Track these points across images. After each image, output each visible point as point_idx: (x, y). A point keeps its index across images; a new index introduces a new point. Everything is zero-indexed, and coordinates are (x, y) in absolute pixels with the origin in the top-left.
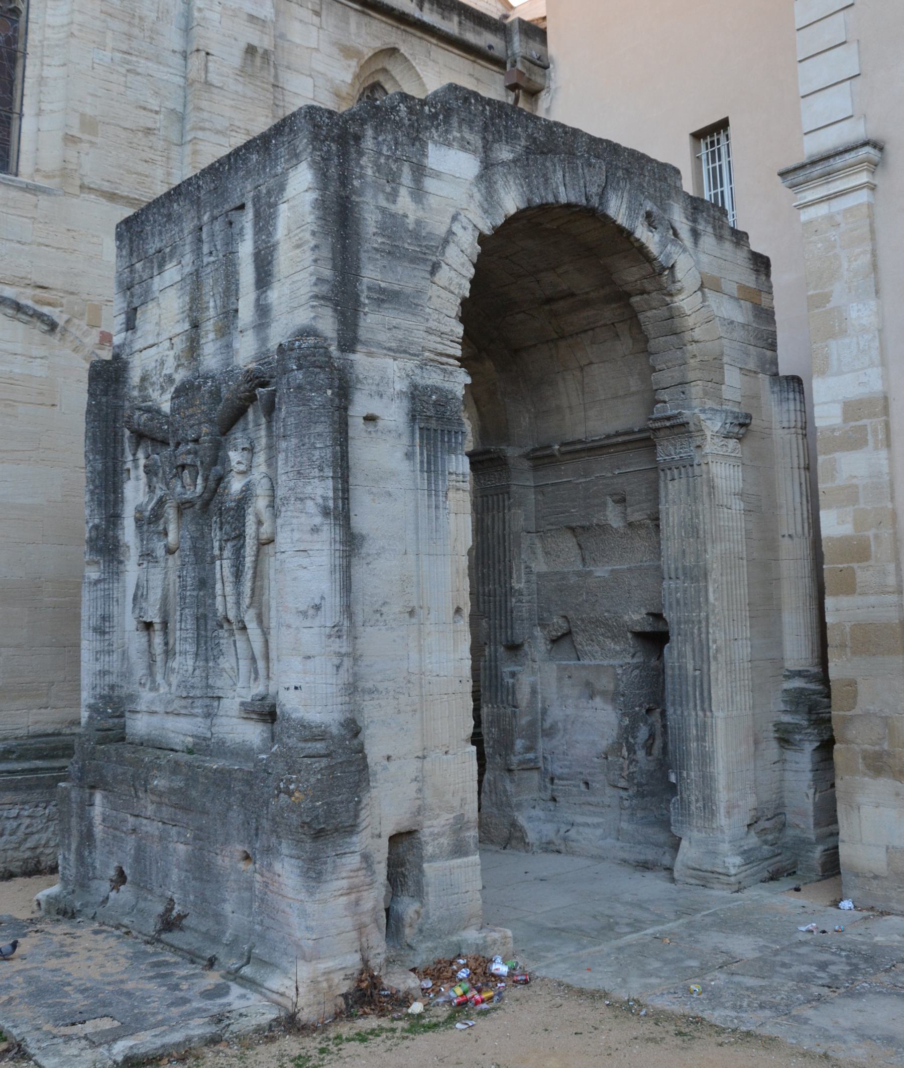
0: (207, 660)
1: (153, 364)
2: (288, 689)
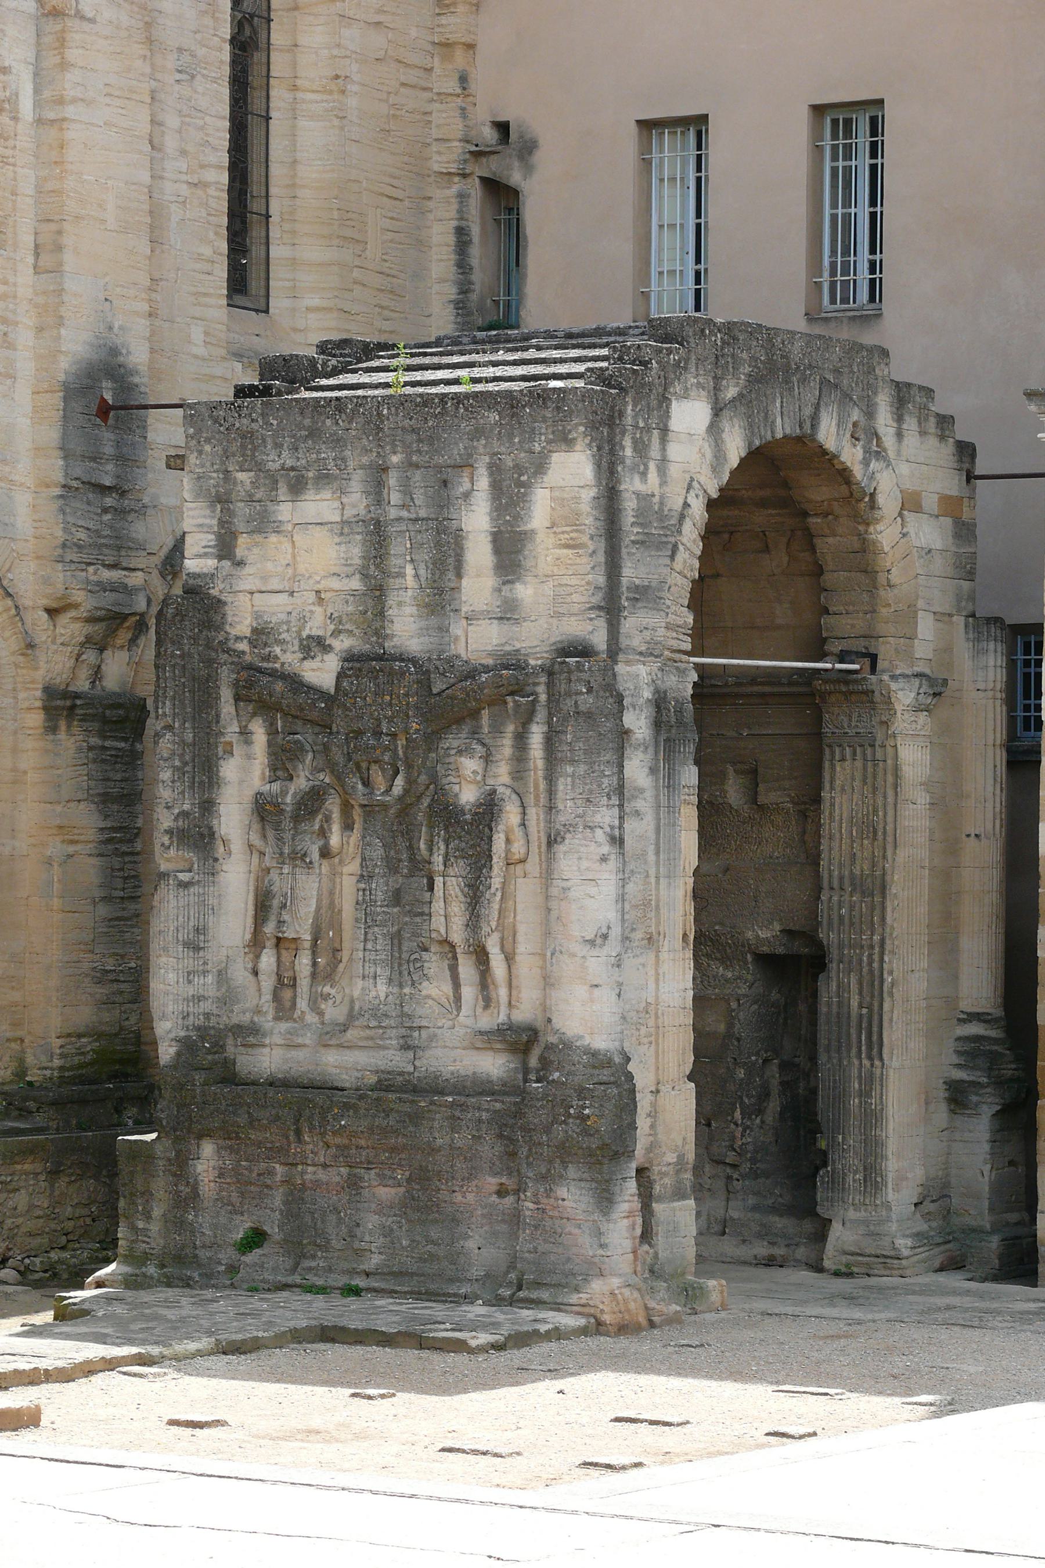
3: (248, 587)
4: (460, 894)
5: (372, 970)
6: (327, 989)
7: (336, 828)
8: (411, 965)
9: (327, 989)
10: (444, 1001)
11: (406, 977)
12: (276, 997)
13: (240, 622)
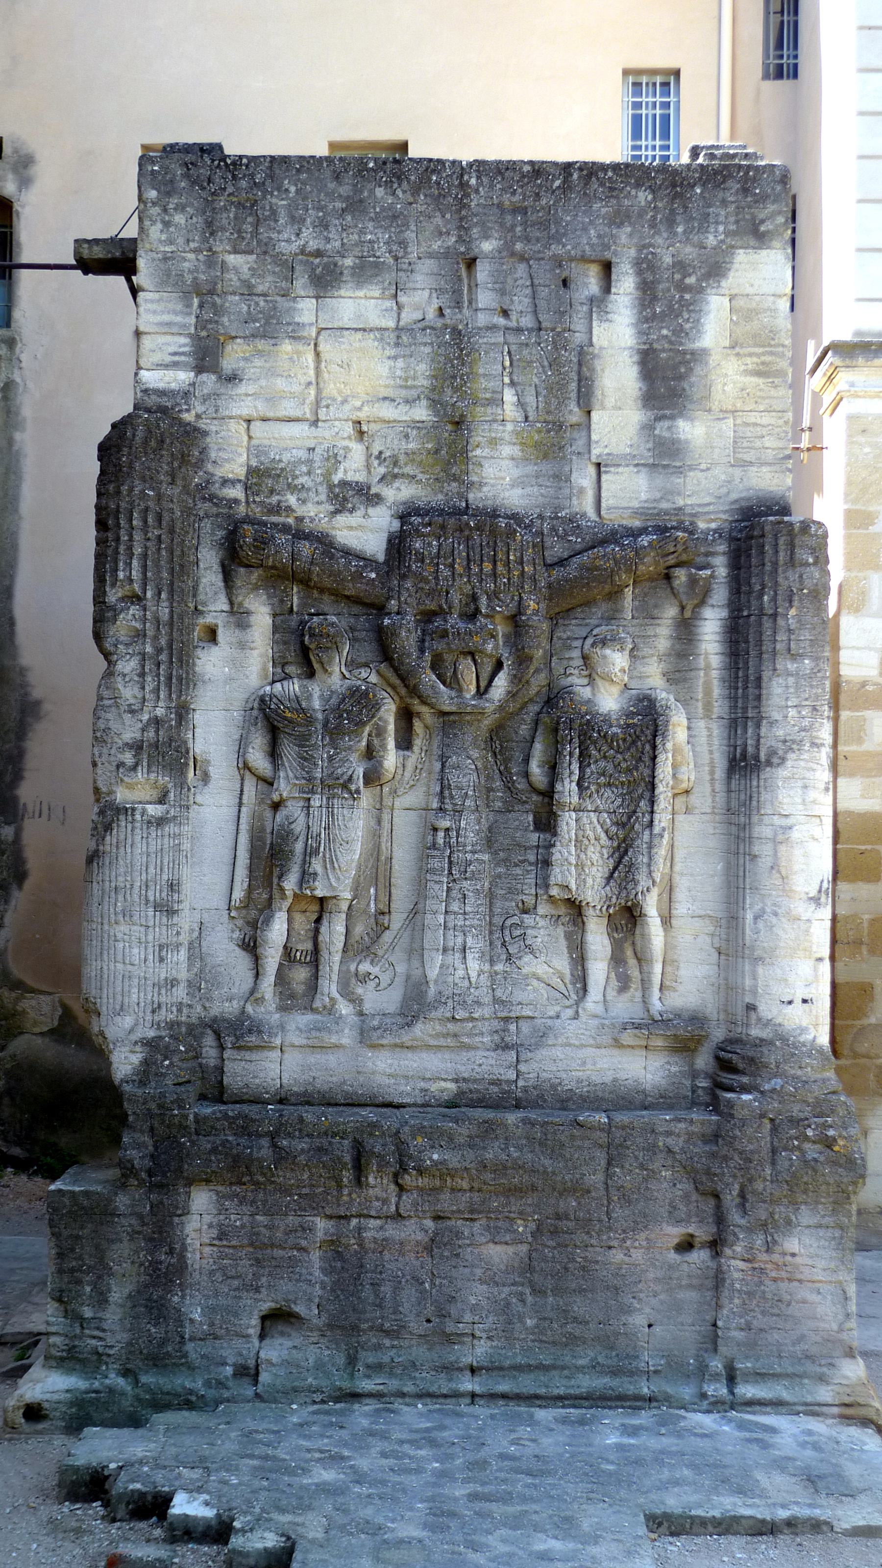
0: (492, 962)
1: (302, 454)
2: (790, 1002)
3: (245, 412)
4: (603, 836)
5: (460, 940)
6: (365, 967)
7: (391, 744)
8: (507, 932)
9: (365, 967)
10: (556, 981)
11: (499, 949)
12: (281, 978)
13: (230, 458)
